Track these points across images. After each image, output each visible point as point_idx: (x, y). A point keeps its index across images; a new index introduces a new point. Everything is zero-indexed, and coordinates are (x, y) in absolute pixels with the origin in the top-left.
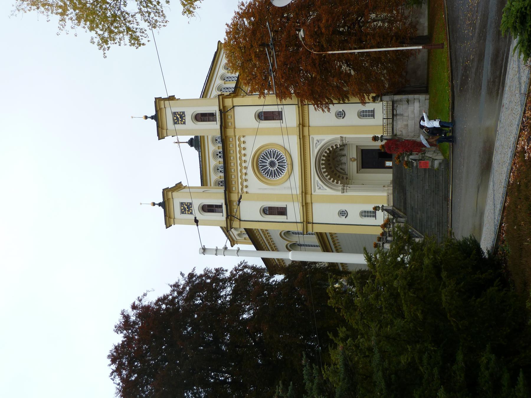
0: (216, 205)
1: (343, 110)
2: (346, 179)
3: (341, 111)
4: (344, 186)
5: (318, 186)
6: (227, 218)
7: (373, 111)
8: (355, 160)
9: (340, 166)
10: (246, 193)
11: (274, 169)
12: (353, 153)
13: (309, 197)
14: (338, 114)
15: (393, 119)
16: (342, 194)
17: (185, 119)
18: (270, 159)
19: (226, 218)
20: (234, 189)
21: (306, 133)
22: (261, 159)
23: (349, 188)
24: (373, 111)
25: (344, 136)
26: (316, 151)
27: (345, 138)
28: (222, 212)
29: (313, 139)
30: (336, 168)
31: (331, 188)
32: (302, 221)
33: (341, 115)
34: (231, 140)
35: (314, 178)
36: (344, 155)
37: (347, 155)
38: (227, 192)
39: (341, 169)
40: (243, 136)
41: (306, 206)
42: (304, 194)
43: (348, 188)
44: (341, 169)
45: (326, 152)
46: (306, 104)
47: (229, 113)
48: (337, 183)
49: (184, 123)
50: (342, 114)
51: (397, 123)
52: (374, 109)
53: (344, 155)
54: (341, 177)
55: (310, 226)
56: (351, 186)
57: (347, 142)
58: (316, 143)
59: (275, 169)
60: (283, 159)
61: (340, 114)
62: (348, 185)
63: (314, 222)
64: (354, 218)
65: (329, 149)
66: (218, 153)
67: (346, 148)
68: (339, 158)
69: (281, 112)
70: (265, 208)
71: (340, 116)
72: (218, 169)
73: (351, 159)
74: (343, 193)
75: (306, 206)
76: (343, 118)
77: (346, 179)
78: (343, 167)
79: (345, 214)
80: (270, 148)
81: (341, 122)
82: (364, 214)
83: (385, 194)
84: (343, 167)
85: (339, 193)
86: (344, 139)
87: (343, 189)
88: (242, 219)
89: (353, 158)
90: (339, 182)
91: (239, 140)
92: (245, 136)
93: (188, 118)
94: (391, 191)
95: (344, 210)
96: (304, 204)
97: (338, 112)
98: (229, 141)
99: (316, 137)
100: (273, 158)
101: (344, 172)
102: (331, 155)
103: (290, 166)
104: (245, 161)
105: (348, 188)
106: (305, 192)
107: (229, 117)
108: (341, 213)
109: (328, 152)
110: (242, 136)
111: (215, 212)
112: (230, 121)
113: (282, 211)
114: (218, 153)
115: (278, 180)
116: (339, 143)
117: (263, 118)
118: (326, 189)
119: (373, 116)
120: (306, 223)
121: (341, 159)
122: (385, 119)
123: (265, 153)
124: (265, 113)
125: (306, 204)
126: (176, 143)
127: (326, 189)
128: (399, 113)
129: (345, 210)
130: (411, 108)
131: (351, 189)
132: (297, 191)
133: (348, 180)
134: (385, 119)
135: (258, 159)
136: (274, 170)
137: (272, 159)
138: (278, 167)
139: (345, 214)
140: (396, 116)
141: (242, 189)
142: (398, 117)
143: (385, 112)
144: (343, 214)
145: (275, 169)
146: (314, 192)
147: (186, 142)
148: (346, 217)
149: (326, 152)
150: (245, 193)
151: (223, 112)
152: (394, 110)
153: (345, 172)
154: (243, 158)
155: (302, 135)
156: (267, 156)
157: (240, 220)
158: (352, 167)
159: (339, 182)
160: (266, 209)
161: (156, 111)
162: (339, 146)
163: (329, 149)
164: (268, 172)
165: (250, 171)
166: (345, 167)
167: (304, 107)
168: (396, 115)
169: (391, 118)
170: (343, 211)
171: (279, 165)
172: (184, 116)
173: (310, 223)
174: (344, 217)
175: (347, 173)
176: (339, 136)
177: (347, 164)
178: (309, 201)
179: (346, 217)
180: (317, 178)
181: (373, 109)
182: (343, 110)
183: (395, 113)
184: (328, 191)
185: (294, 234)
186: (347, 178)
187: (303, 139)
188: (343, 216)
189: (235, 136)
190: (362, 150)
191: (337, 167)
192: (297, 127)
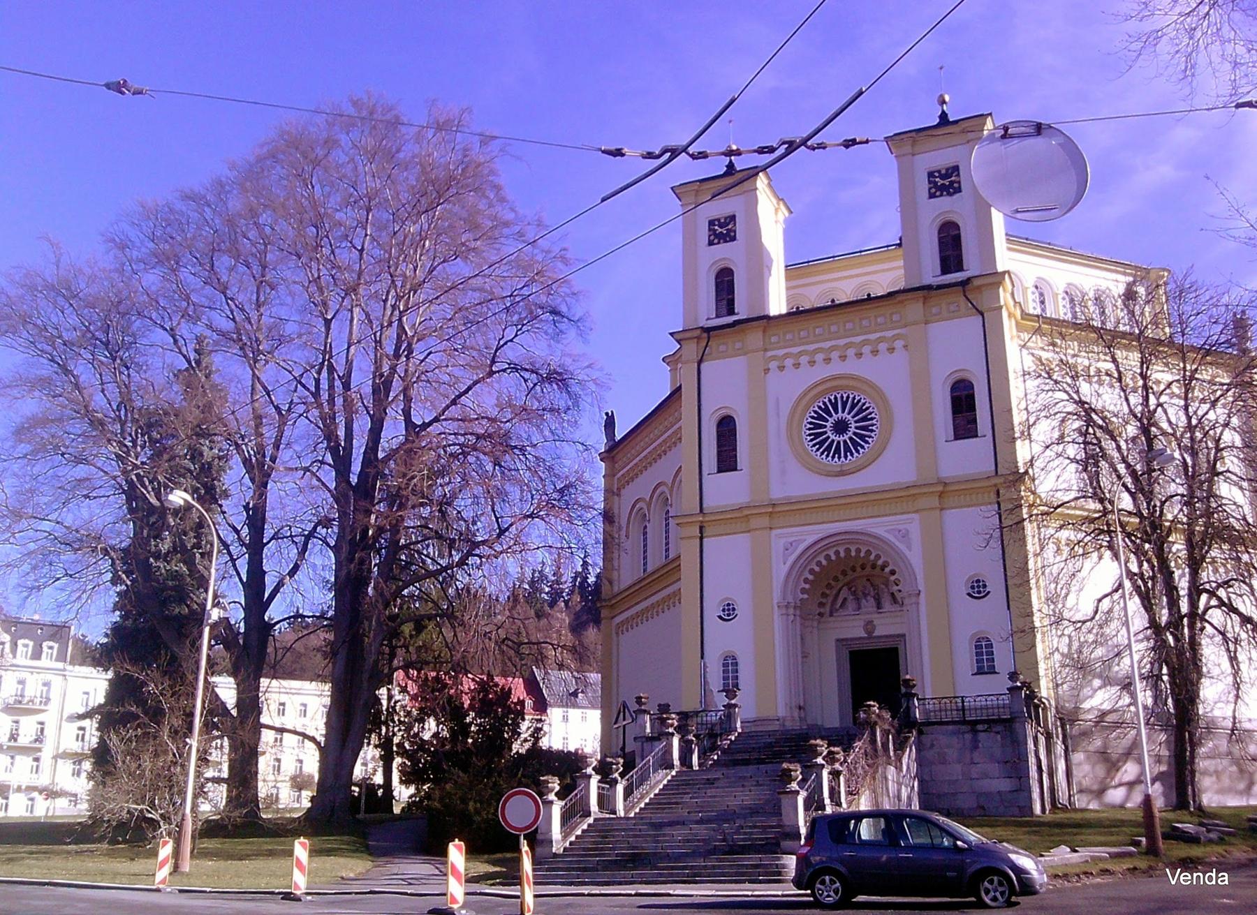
0: (733, 300)
2: (819, 614)
3: (988, 590)
7: (992, 671)
8: (870, 633)
12: (886, 626)
15: (964, 722)
17: (941, 195)
18: (849, 417)
19: (702, 328)
21: (923, 503)
24: (992, 671)
26: (880, 531)
27: (918, 603)
28: (717, 316)
35: (810, 534)
36: (879, 606)
39: (845, 599)
41: (739, 518)
44: (845, 599)
45: (878, 557)
48: (803, 591)
49: (932, 196)
50: (979, 592)
51: (954, 733)
53: (879, 606)
54: (824, 601)
56: (798, 624)
59: (829, 434)
61: (978, 587)
63: (705, 540)
64: (722, 639)
67: (897, 607)
69: (977, 436)
71: (973, 587)
73: (870, 622)
75: (739, 518)
76: (969, 594)
77: (819, 614)
78: (851, 605)
79: (729, 615)
80: (880, 417)
81: (959, 589)
82: (730, 665)
83: (781, 712)
84: (851, 605)
86: (914, 600)
88: (703, 366)
89: (874, 628)
90: (806, 596)
93: (945, 205)
94: (789, 725)
96: (746, 512)
101: (838, 606)
108: (728, 605)
113: (727, 462)
119: (980, 672)
120: (702, 522)
121: (869, 598)
122: (963, 702)
124: (971, 398)
130: (994, 769)
132: (778, 492)
133: (817, 617)
134: (963, 702)
141: (774, 358)
142: (968, 736)
143: (981, 702)
144: (729, 610)
152: (986, 726)
153: (837, 610)
157: (700, 362)
158: (851, 627)
161: (956, 122)
165: (822, 372)
166: (850, 609)
171: (839, 442)
172: (950, 194)
173: (701, 532)
178: (755, 523)
179: (720, 617)
180: (811, 540)
183: (980, 727)
184: (780, 570)
186: (821, 615)
191: (850, 589)
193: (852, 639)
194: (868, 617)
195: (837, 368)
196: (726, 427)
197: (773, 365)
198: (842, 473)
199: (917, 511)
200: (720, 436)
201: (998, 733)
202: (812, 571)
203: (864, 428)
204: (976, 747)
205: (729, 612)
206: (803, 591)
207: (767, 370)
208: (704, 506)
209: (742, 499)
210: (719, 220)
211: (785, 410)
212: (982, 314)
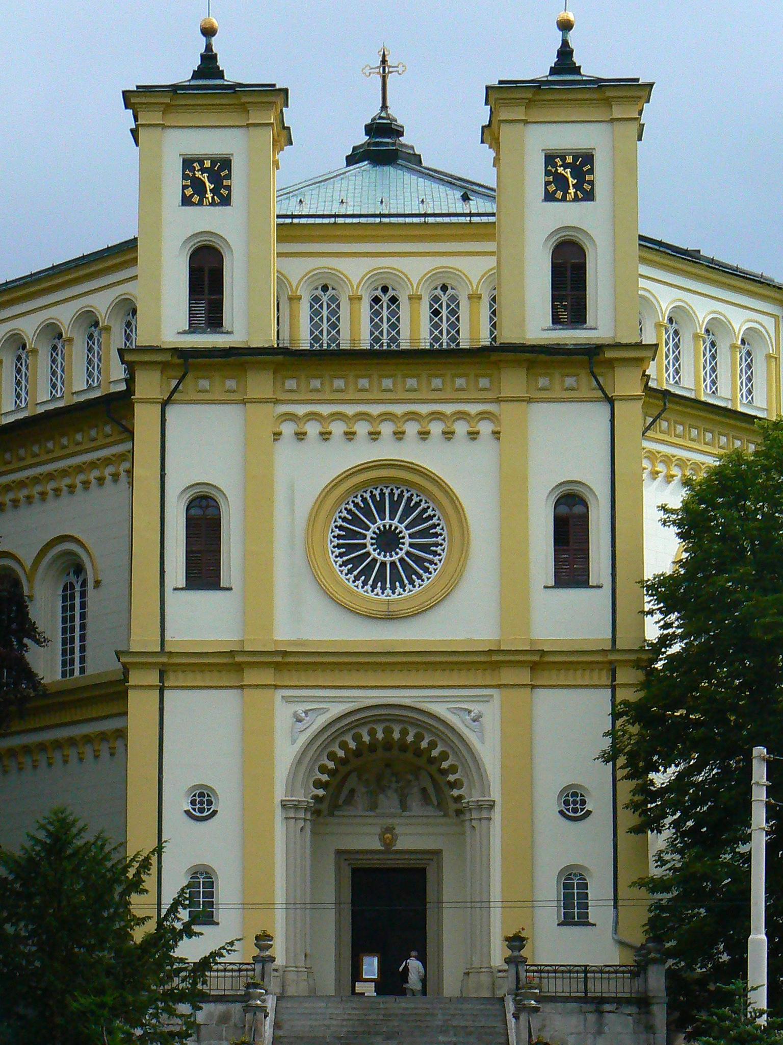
0: (220, 303)
1: (589, 813)
3: (588, 807)
4: (306, 810)
5: (306, 712)
6: (178, 352)
7: (584, 921)
9: (363, 790)
10: (275, 434)
11: (369, 545)
13: (267, 677)
14: (575, 794)
16: (277, 801)
20: (291, 384)
21: (508, 676)
22: (406, 495)
23: (302, 829)
24: (584, 921)
25: (497, 815)
26: (440, 709)
27: (489, 819)
28: (193, 328)
29: (487, 699)
30: (354, 776)
31: (299, 761)
32: (167, 649)
34: (484, 382)
36: (404, 806)
37: (405, 814)
38: (280, 357)
40: (499, 433)
42: (279, 659)
43: (301, 823)
44: (352, 791)
45: (433, 745)
46: (614, 679)
47: (586, 386)
48: (318, 784)
50: (575, 811)
52: (595, 925)
53: (404, 806)
55: (153, 678)
57: (474, 823)
58: (470, 712)
59: (370, 548)
60: (406, 582)
61: (575, 803)
62: (308, 823)
63: (167, 693)
65: (444, 756)
66: (391, 293)
68: (394, 785)
70: (212, 503)
71: (566, 803)
72: (325, 288)
73: (389, 829)
74: (284, 806)
76: (561, 812)
79: (201, 810)
85: (280, 793)
86: (485, 814)
87: (296, 807)
88: (171, 411)
89: (395, 838)
90: (321, 792)
91: (484, 416)
92: (498, 439)
95: (213, 808)
96: (238, 659)
97: (582, 795)
98: (477, 376)
100: (411, 545)
101: (340, 802)
102: (433, 769)
103: (385, 608)
104: (399, 435)
105: (301, 823)
107: (570, 381)
108: (201, 795)
109: (435, 753)
110: (498, 429)
111: (190, 300)
114: (391, 293)
115: (327, 559)
116: (472, 795)
117: (563, 510)
118: (294, 742)
119: (567, 921)
120: (163, 664)
121: (390, 793)
123: (430, 512)
125: (239, 668)
126: (384, 61)
127: (294, 742)
128: (607, 1021)
129: (215, 812)
131: (298, 835)
135: (410, 484)
136: (365, 546)
137: (407, 540)
138: (375, 560)
139: (201, 810)
140: (596, 1011)
141: (290, 417)
142: (591, 1018)
145: (370, 548)
146: (283, 697)
147: (384, 107)
148: (187, 812)
149: (433, 745)
150: (277, 430)
154: (412, 429)
155: (503, 662)
156: (419, 520)
159: (321, 792)
160: (207, 507)
162: (455, 793)
163: (444, 756)
164: (356, 520)
167: (604, 673)
168: (601, 1013)
169: (586, 992)
170: (210, 803)
173: (161, 680)
174: (189, 807)
175: (336, 813)
176: (495, 794)
177: (372, 814)
178: (250, 677)
179: (187, 812)
180: (337, 710)
181: (591, 920)
182: (589, 813)
183: (607, 1007)
185: (65, 589)
188: (193, 803)
189: (498, 400)
190: (423, 871)
191: (360, 777)
192: (532, 642)
193: (358, 852)
194: (390, 821)
197: (288, 429)
198: (390, 617)
199: (498, 686)
200: (192, 525)
201: (630, 1015)
202: (332, 756)
203: (424, 548)
204: (599, 1032)
206: (318, 784)
207: (277, 435)
208: (168, 638)
210: (201, 162)
211: (305, 505)
212: (611, 401)
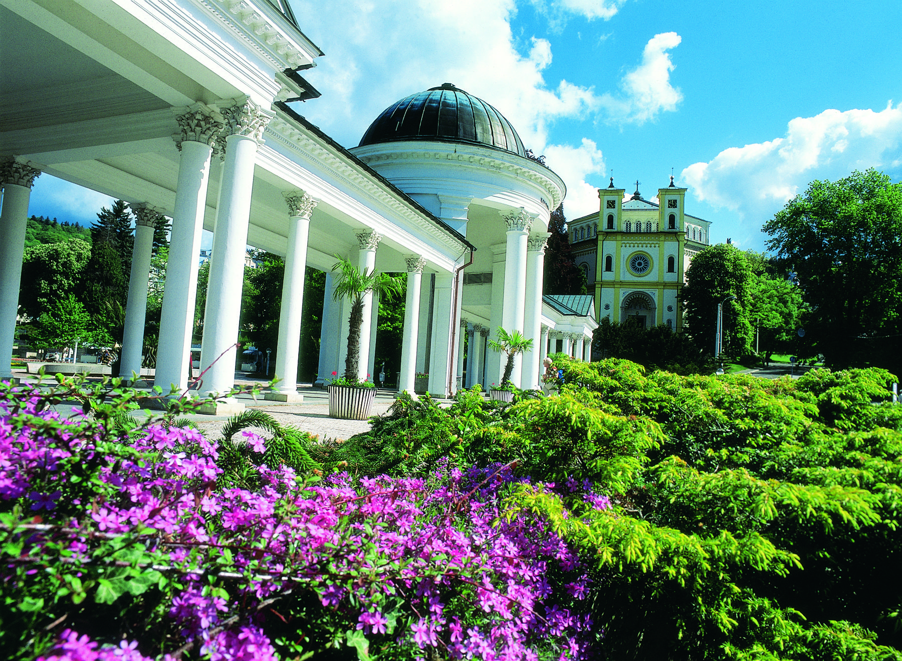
33: (670, 309)
35: (631, 291)
41: (613, 284)
75: (613, 284)
81: (666, 309)
93: (672, 210)
99: (657, 292)
106: (622, 284)
112: (670, 237)
151: (676, 233)
165: (637, 249)
178: (616, 286)
187: (655, 284)
195: (640, 249)
196: (609, 259)
205: (607, 307)
209: (612, 279)
